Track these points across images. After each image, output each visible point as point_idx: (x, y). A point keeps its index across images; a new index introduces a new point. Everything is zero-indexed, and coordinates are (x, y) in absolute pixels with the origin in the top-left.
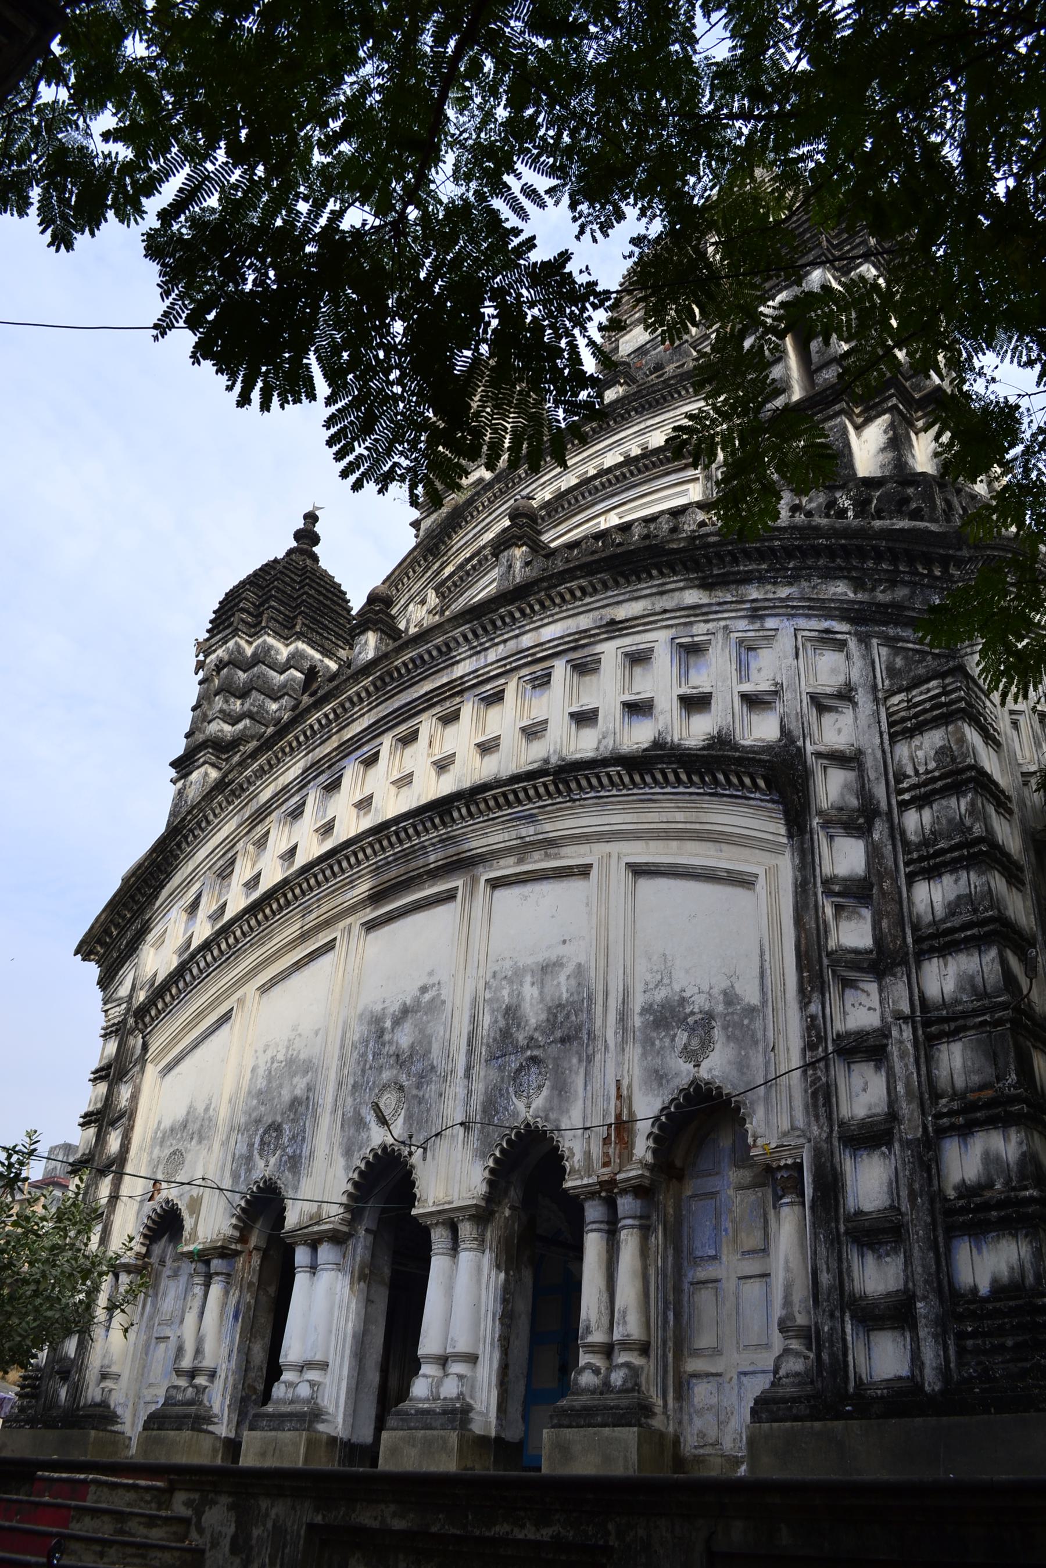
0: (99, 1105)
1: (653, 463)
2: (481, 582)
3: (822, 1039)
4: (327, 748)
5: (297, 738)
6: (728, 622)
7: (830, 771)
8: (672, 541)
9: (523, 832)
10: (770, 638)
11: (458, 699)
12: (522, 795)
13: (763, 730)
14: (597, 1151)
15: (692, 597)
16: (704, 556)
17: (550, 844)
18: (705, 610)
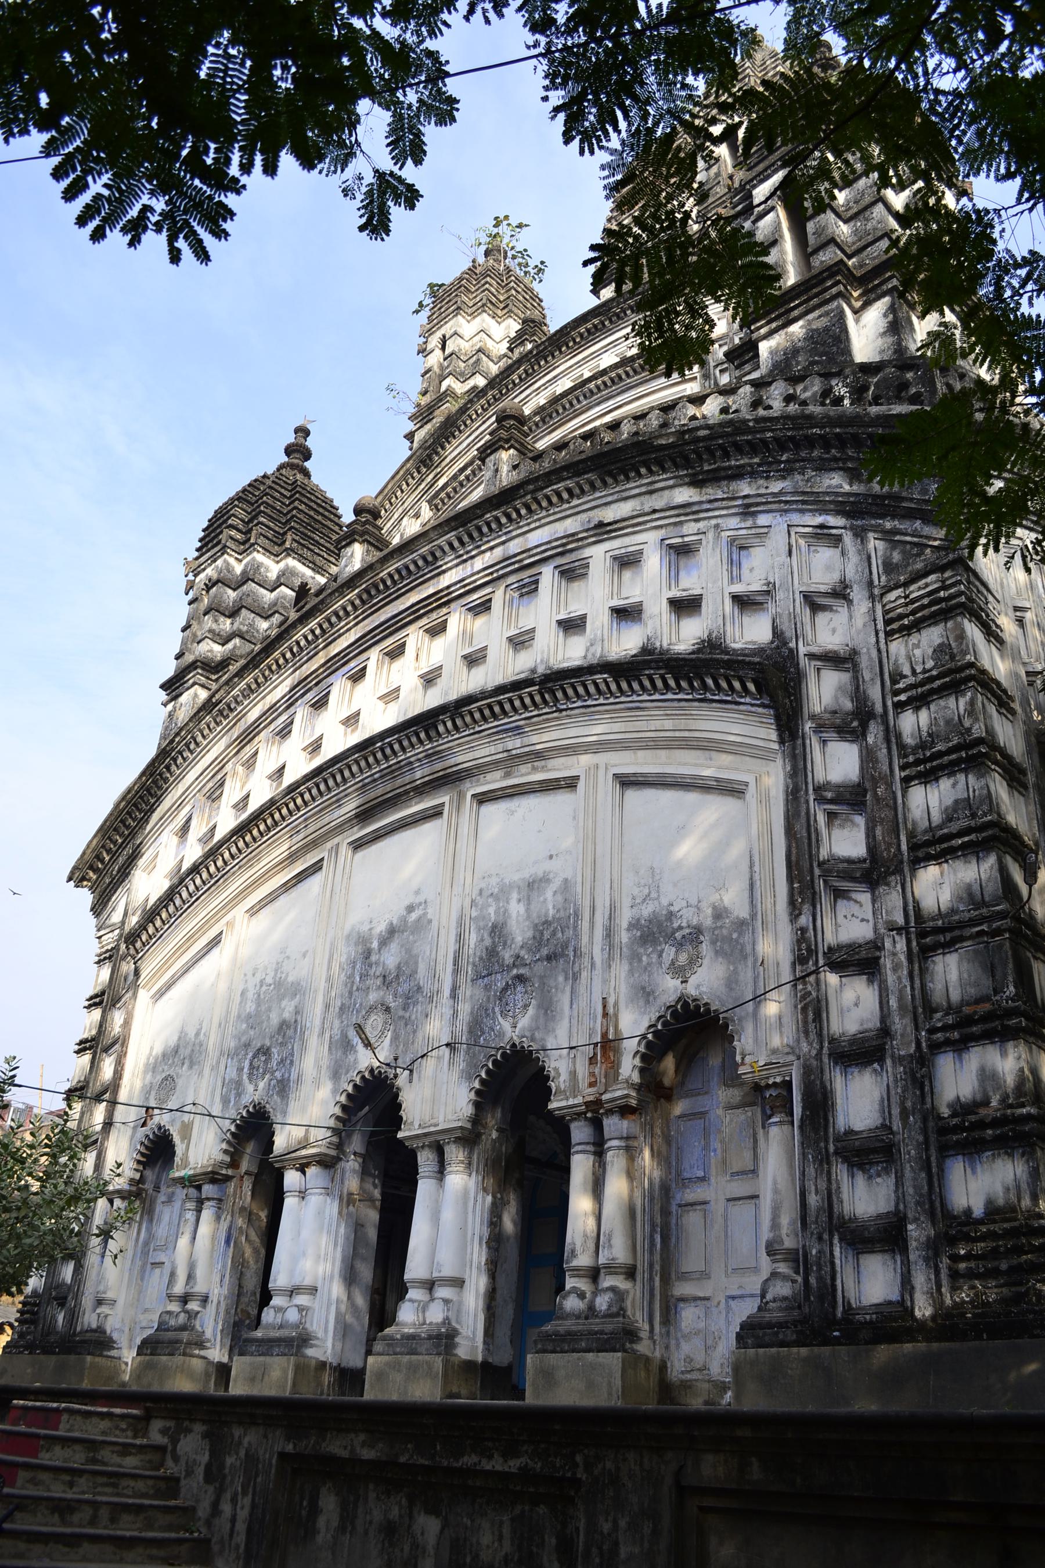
0: (94, 1032)
3: (812, 952)
5: (284, 656)
6: (720, 521)
7: (823, 672)
8: (661, 436)
9: (510, 745)
10: (762, 535)
11: (445, 610)
12: (507, 707)
13: (753, 633)
14: (582, 1069)
15: (684, 495)
16: (694, 451)
17: (538, 756)
18: (695, 508)
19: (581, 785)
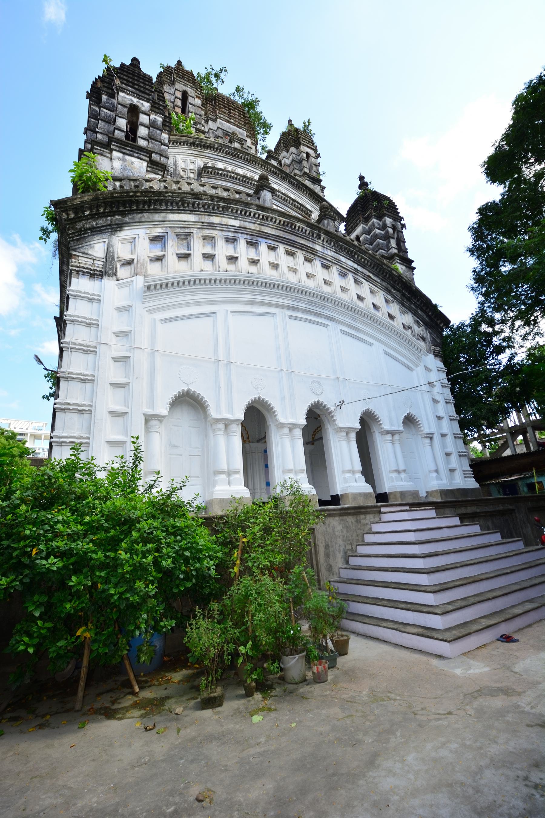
4: (252, 226)
11: (312, 256)
19: (373, 346)
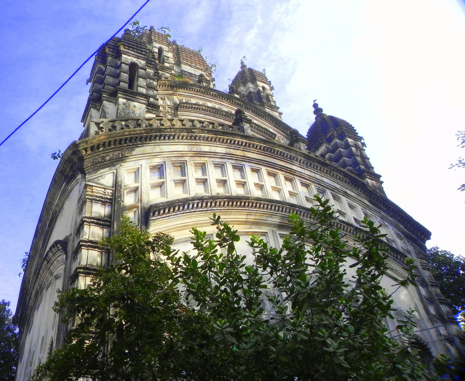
1: (262, 131)
2: (194, 114)
11: (292, 176)
